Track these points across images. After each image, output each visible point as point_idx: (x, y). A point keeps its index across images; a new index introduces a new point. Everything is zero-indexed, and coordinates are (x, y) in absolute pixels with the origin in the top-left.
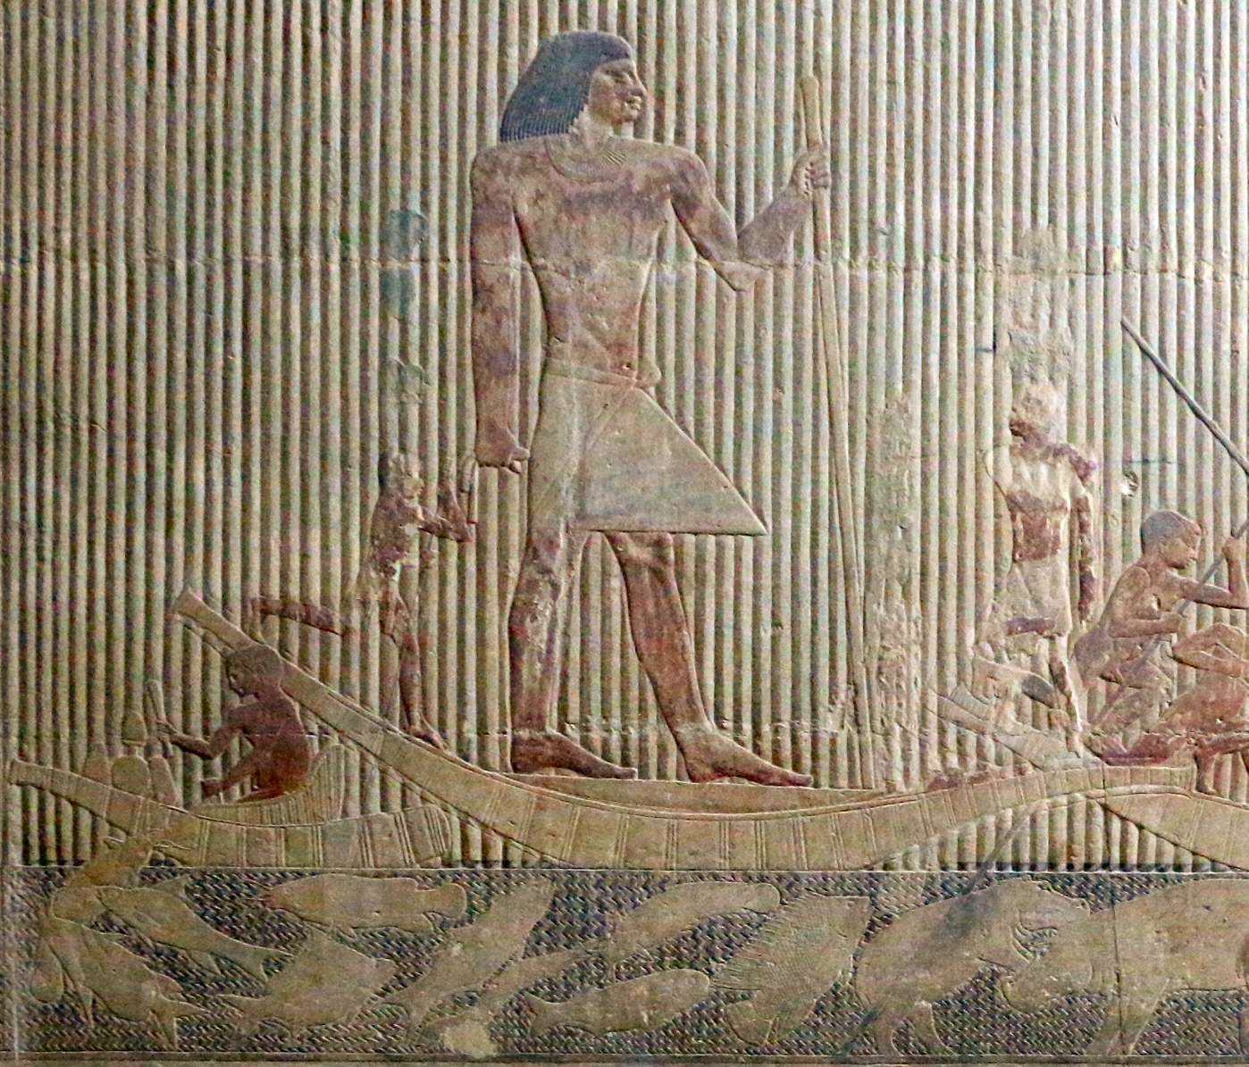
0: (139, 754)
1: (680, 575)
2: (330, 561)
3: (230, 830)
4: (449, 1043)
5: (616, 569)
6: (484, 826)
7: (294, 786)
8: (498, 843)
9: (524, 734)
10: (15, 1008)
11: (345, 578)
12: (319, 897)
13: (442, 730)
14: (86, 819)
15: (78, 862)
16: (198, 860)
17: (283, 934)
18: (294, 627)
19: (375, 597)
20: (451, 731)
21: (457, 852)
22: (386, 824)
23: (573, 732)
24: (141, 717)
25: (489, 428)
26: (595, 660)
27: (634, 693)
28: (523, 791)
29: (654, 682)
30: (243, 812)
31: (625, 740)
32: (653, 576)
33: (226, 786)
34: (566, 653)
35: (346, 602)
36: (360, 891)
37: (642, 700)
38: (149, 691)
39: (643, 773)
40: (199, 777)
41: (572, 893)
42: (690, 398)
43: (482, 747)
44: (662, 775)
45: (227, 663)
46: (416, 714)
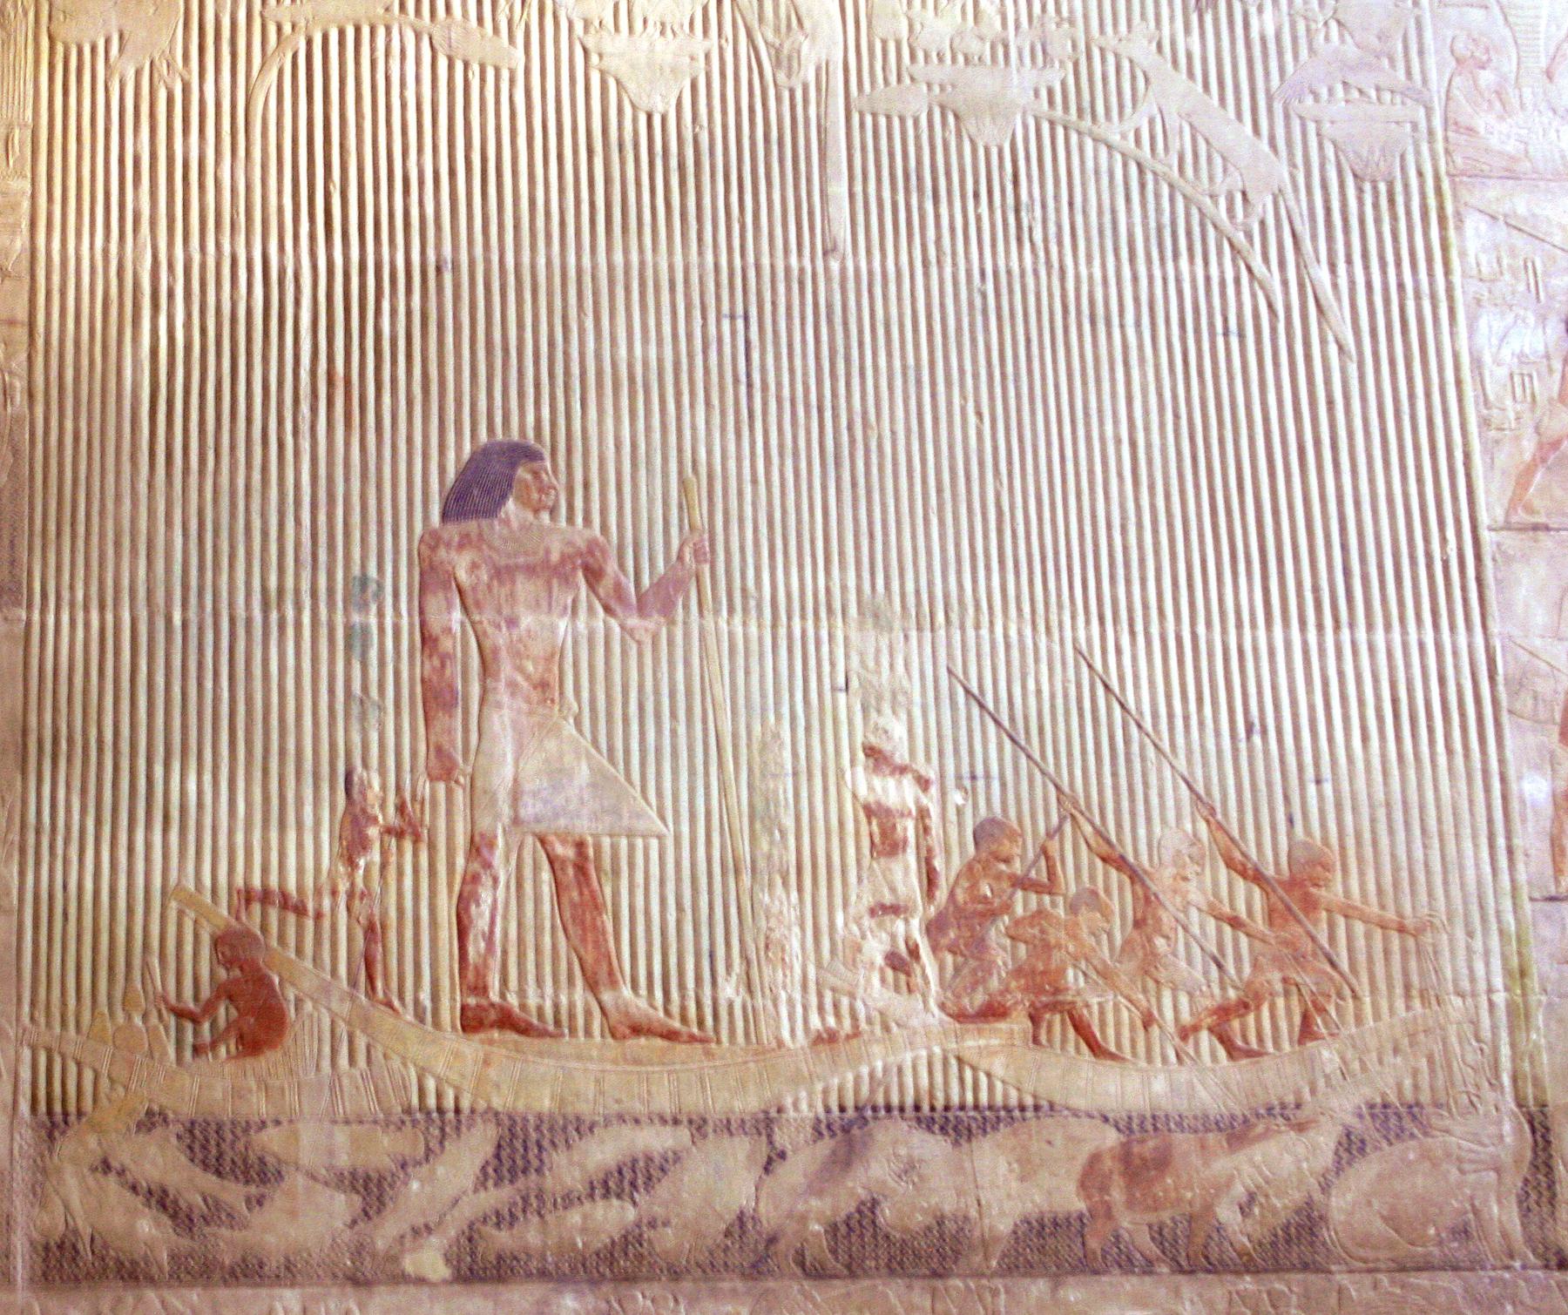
0: (138, 1020)
2: (306, 855)
3: (216, 1084)
7: (272, 1045)
9: (472, 1001)
10: (20, 1244)
12: (295, 1135)
13: (401, 998)
14: (88, 1076)
15: (80, 1113)
16: (187, 1110)
17: (261, 1174)
19: (343, 887)
21: (415, 1101)
22: (351, 1077)
24: (139, 986)
28: (471, 1048)
29: (580, 959)
30: (229, 1068)
31: (556, 1006)
32: (578, 873)
33: (214, 1045)
35: (318, 892)
36: (331, 1135)
38: (146, 965)
41: (513, 1135)
45: (216, 942)
46: (379, 984)
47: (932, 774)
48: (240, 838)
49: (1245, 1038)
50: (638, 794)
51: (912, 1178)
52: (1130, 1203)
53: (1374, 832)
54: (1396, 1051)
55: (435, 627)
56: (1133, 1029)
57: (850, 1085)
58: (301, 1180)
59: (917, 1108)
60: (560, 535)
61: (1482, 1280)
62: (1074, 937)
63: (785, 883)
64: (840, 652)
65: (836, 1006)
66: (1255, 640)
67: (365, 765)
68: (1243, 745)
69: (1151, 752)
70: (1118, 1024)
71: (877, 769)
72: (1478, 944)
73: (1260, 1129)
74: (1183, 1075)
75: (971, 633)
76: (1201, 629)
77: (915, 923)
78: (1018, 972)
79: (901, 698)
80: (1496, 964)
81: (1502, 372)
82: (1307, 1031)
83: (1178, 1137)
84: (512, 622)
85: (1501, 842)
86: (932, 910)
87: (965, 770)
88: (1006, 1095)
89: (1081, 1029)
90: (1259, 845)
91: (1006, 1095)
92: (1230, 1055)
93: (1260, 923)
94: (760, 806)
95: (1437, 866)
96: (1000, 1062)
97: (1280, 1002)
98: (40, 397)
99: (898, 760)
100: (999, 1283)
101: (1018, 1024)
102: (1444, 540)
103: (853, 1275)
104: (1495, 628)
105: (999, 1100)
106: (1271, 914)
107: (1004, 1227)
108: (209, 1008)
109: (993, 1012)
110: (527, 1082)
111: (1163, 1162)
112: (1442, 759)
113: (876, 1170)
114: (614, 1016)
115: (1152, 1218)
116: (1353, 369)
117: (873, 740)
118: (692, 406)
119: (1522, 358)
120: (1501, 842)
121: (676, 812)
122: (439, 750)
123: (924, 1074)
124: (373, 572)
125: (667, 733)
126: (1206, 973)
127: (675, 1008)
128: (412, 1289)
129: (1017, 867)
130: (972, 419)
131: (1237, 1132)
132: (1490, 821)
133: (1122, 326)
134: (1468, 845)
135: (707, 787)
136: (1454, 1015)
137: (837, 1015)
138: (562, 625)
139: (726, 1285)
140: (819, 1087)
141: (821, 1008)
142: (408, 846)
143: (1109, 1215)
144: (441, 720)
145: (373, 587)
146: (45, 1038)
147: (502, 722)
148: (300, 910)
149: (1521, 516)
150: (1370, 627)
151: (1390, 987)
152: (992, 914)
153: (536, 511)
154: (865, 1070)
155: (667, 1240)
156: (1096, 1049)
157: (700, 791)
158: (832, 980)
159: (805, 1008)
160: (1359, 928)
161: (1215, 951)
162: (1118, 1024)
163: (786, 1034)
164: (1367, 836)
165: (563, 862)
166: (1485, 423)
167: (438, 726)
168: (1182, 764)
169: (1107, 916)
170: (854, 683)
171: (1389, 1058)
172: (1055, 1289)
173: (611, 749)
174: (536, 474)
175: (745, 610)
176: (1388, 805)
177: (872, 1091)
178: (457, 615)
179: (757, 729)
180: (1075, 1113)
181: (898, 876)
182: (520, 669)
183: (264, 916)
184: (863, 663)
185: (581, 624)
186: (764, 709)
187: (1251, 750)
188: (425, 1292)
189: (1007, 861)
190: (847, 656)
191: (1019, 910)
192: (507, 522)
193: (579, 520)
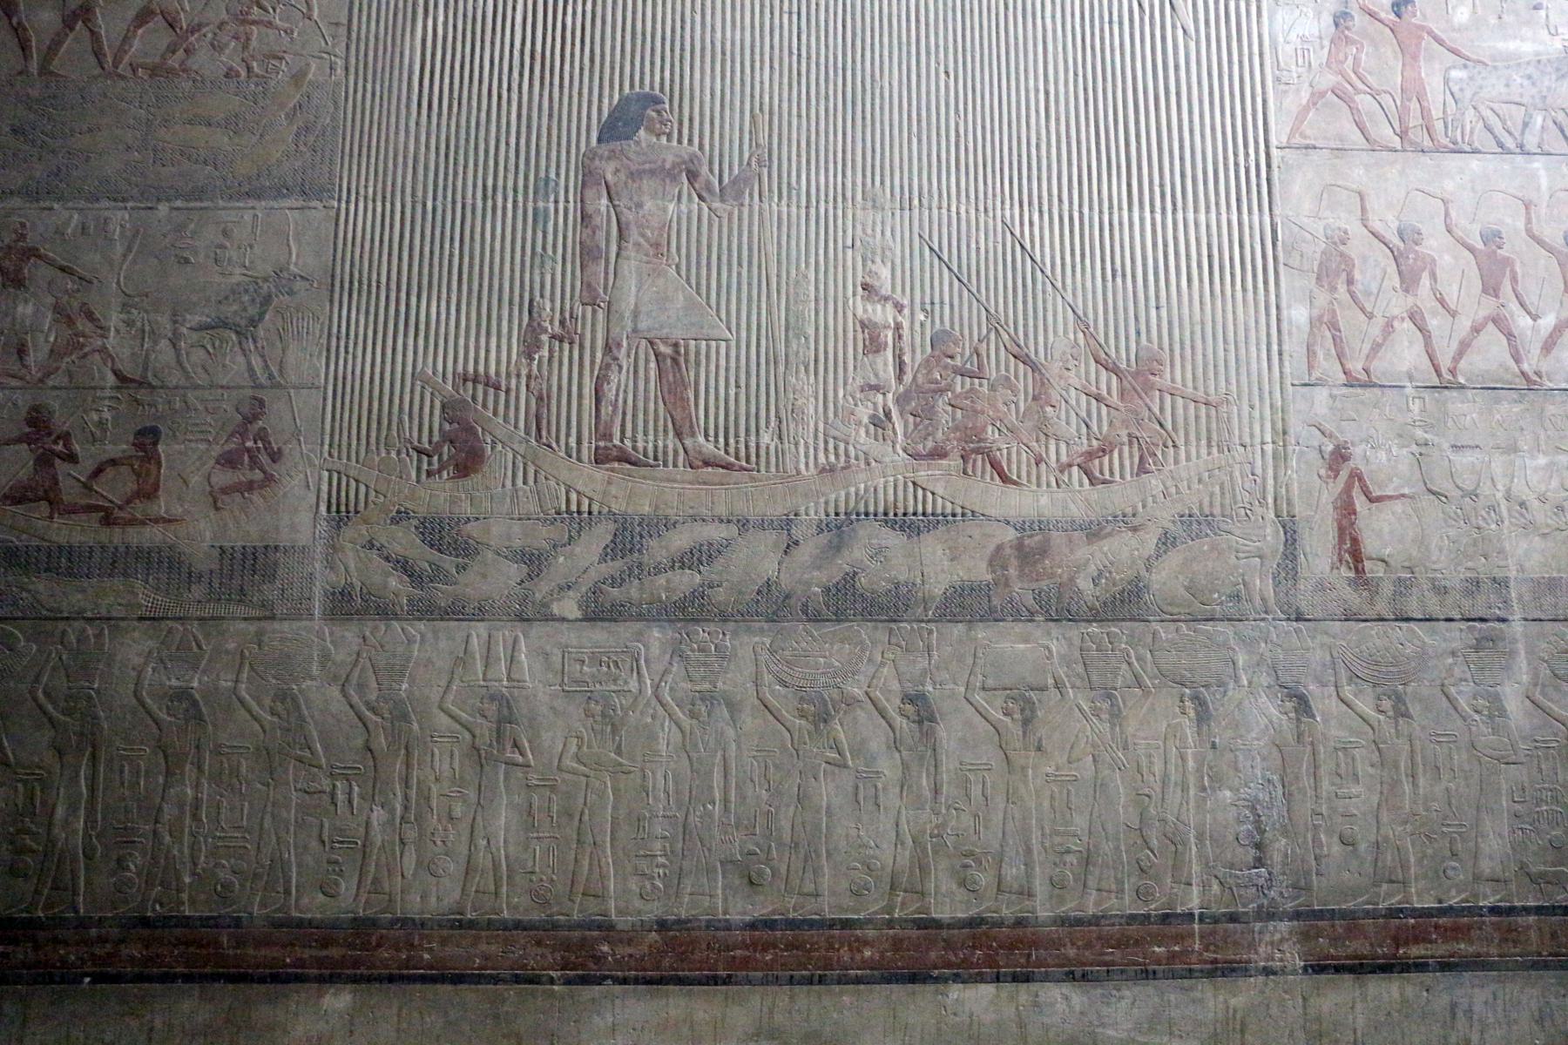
0: (393, 455)
1: (686, 361)
2: (500, 352)
3: (440, 495)
4: (556, 611)
5: (653, 358)
6: (579, 493)
7: (476, 471)
8: (587, 502)
9: (602, 444)
10: (317, 592)
11: (509, 362)
13: (558, 442)
14: (363, 489)
16: (422, 511)
17: (465, 550)
18: (480, 388)
19: (524, 372)
20: (563, 442)
21: (564, 507)
23: (628, 443)
25: (588, 286)
26: (641, 405)
27: (661, 422)
28: (600, 474)
30: (448, 485)
31: (656, 447)
32: (673, 363)
33: (439, 471)
34: (625, 402)
35: (508, 375)
37: (665, 426)
39: (665, 465)
40: (425, 466)
41: (625, 529)
42: (694, 270)
43: (579, 451)
44: (675, 465)
45: (443, 407)
46: (544, 433)
47: (906, 302)
48: (462, 342)
49: (1102, 473)
50: (714, 313)
51: (882, 558)
52: (1020, 577)
53: (1192, 341)
54: (1200, 481)
55: (590, 209)
56: (1029, 465)
57: (843, 498)
58: (490, 555)
59: (886, 514)
60: (671, 151)
61: (1246, 628)
62: (993, 406)
63: (807, 370)
64: (849, 223)
65: (836, 448)
66: (1120, 217)
67: (542, 296)
68: (1110, 284)
69: (1049, 288)
70: (1019, 462)
71: (868, 299)
72: (1256, 414)
73: (1109, 529)
74: (1060, 495)
75: (935, 211)
76: (1086, 210)
77: (890, 396)
78: (956, 428)
79: (888, 253)
80: (1268, 426)
81: (1289, 49)
82: (1142, 469)
83: (1054, 534)
84: (639, 205)
85: (1275, 347)
86: (901, 388)
87: (928, 300)
88: (944, 507)
89: (995, 465)
90: (1117, 348)
91: (944, 507)
92: (1092, 484)
93: (1115, 399)
94: (792, 320)
95: (1232, 363)
96: (943, 484)
97: (1126, 449)
98: (352, 70)
99: (883, 292)
100: (932, 626)
101: (954, 462)
102: (1247, 155)
103: (839, 621)
104: (1277, 211)
105: (939, 511)
106: (1122, 394)
107: (938, 591)
108: (437, 448)
109: (938, 454)
110: (633, 495)
111: (1044, 550)
112: (1239, 294)
113: (857, 553)
114: (691, 453)
115: (1034, 585)
116: (1192, 45)
117: (868, 280)
118: (761, 69)
119: (1303, 39)
120: (1275, 347)
121: (738, 325)
122: (589, 285)
123: (891, 491)
124: (553, 175)
125: (735, 275)
126: (1078, 431)
127: (732, 450)
128: (557, 624)
129: (958, 362)
130: (943, 76)
131: (1094, 532)
132: (1268, 335)
133: (1043, 18)
134: (1253, 349)
135: (759, 308)
136: (1238, 459)
137: (837, 455)
138: (671, 207)
139: (757, 625)
140: (822, 500)
141: (826, 449)
142: (566, 346)
143: (1007, 585)
144: (592, 268)
145: (552, 184)
146: (337, 466)
147: (630, 267)
148: (497, 388)
149: (1297, 140)
150: (1196, 211)
151: (1198, 439)
152: (942, 391)
153: (658, 136)
154: (853, 490)
155: (720, 595)
156: (1005, 479)
157: (755, 311)
158: (833, 432)
159: (816, 449)
160: (1180, 401)
161: (1084, 414)
162: (1019, 462)
163: (802, 467)
164: (1188, 343)
165: (664, 356)
166: (1277, 80)
167: (588, 271)
168: (1070, 298)
169: (1015, 393)
170: (858, 243)
171: (1196, 486)
172: (970, 629)
173: (698, 284)
174: (658, 112)
175: (789, 198)
176: (1203, 323)
177: (857, 502)
178: (604, 201)
179: (793, 272)
180: (988, 518)
181: (880, 366)
182: (643, 236)
183: (475, 389)
184: (864, 230)
185: (683, 207)
186: (798, 259)
187: (1114, 287)
188: (565, 625)
189: (952, 357)
190: (854, 227)
191: (959, 389)
192: (638, 143)
193: (685, 141)
